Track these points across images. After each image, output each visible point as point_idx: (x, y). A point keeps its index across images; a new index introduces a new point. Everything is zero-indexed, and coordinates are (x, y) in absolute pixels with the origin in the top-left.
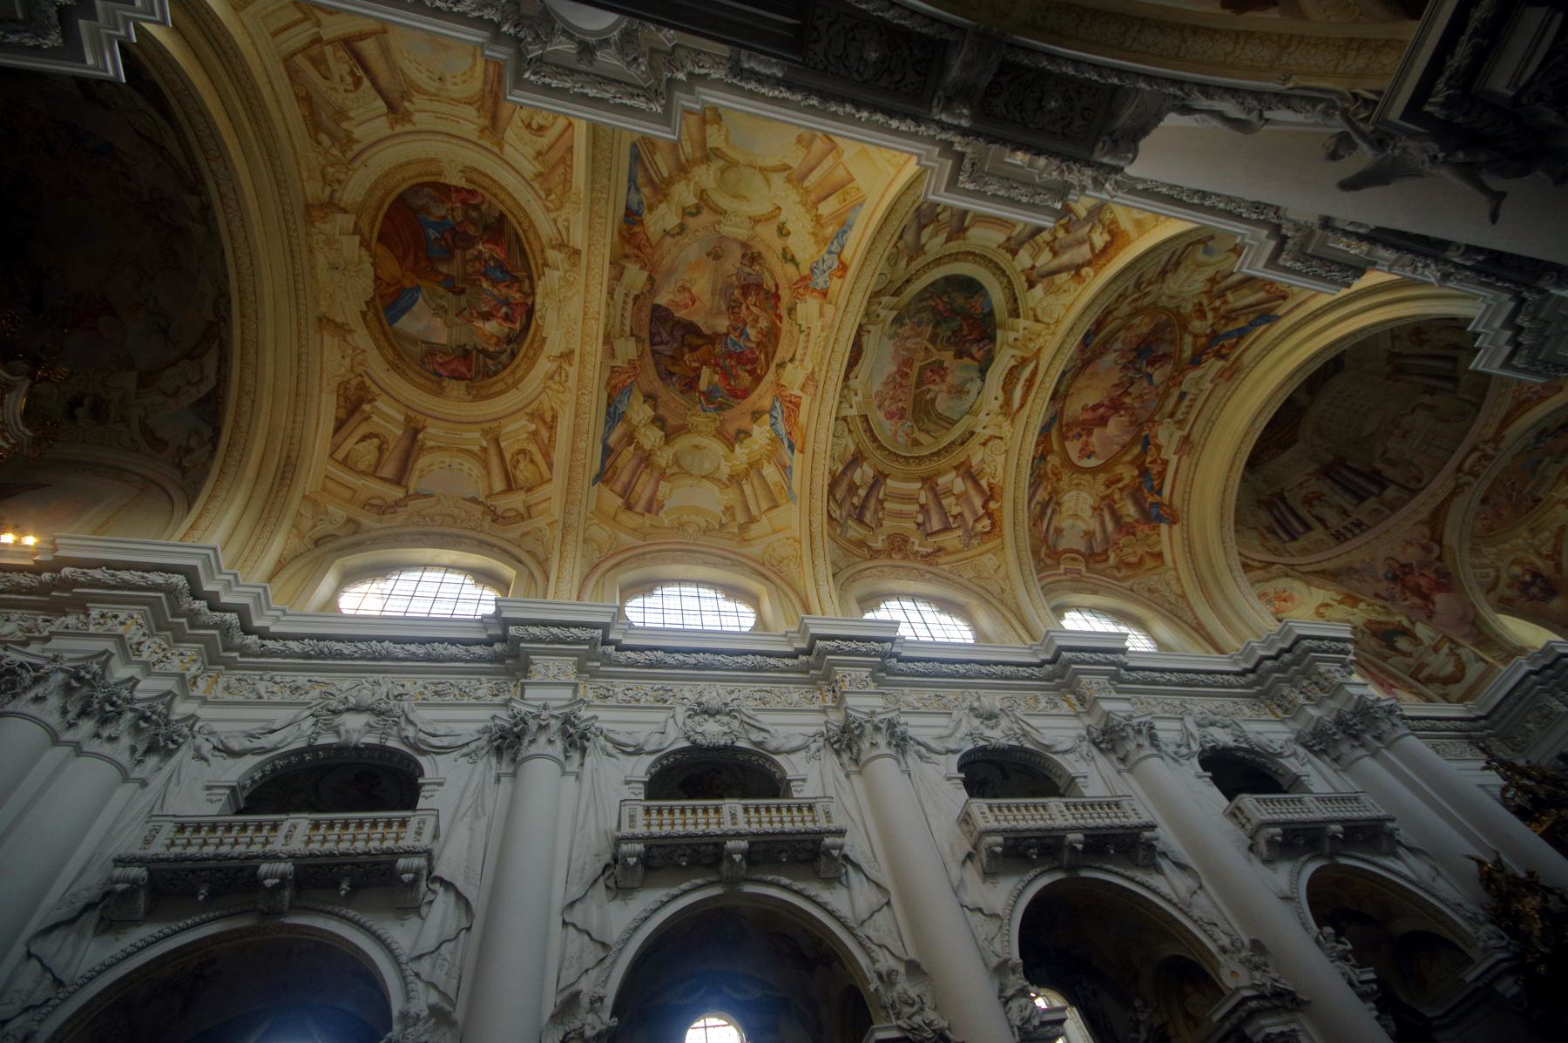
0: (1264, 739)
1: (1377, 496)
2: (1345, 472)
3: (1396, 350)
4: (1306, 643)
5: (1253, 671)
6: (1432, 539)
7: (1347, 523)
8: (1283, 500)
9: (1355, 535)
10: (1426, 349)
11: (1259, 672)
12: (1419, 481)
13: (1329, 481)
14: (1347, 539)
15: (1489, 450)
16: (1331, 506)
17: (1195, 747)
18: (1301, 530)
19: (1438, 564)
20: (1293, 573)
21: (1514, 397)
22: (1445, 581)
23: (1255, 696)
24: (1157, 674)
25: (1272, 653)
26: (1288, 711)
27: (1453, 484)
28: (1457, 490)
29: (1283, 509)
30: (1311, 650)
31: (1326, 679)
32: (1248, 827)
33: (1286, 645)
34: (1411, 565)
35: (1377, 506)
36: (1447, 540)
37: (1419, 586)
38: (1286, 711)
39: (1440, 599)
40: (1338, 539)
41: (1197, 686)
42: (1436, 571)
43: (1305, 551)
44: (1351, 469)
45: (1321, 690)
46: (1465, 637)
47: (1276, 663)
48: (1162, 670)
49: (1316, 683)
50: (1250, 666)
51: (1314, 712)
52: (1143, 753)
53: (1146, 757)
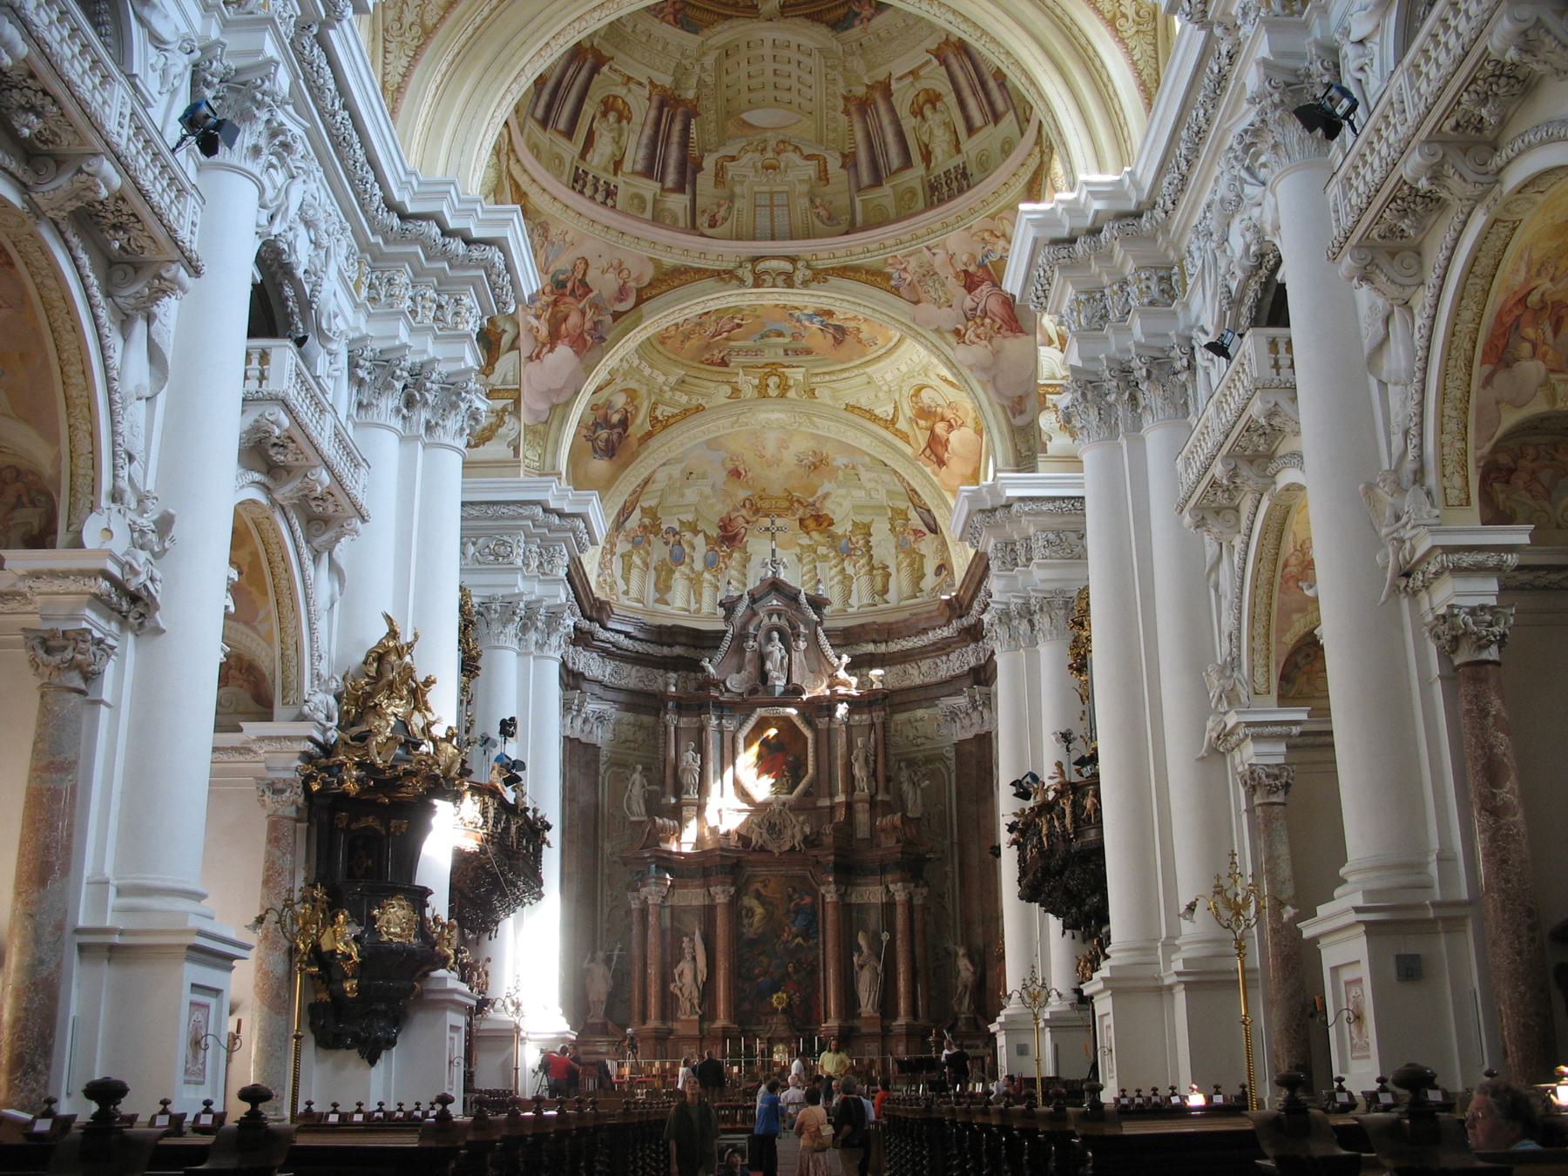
0: (332, 307)
1: (663, 189)
2: (677, 127)
3: (894, 86)
4: (497, 256)
5: (404, 217)
6: (639, 291)
7: (605, 177)
8: (595, 70)
9: (592, 198)
10: (909, 123)
11: (410, 226)
12: (713, 225)
13: (653, 114)
14: (581, 192)
15: (799, 277)
16: (616, 141)
17: (276, 230)
18: (562, 125)
19: (609, 319)
20: (504, 158)
21: (886, 259)
22: (590, 344)
23: (364, 246)
24: (332, 87)
25: (452, 224)
26: (376, 297)
27: (731, 266)
28: (725, 276)
29: (584, 73)
30: (488, 267)
31: (457, 314)
32: (253, 385)
33: (476, 233)
34: (588, 290)
35: (649, 197)
36: (645, 307)
37: (565, 319)
38: (372, 300)
39: (563, 351)
40: (576, 181)
41: (342, 161)
42: (595, 323)
43: (535, 149)
44: (686, 130)
45: (436, 319)
46: (530, 410)
47: (440, 241)
48: (343, 90)
49: (440, 307)
50: (411, 208)
51: (404, 336)
52: (249, 165)
53: (249, 175)
